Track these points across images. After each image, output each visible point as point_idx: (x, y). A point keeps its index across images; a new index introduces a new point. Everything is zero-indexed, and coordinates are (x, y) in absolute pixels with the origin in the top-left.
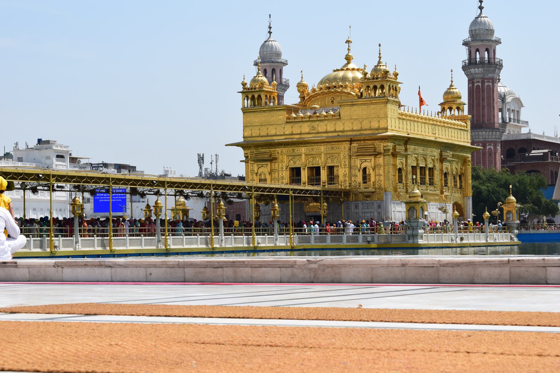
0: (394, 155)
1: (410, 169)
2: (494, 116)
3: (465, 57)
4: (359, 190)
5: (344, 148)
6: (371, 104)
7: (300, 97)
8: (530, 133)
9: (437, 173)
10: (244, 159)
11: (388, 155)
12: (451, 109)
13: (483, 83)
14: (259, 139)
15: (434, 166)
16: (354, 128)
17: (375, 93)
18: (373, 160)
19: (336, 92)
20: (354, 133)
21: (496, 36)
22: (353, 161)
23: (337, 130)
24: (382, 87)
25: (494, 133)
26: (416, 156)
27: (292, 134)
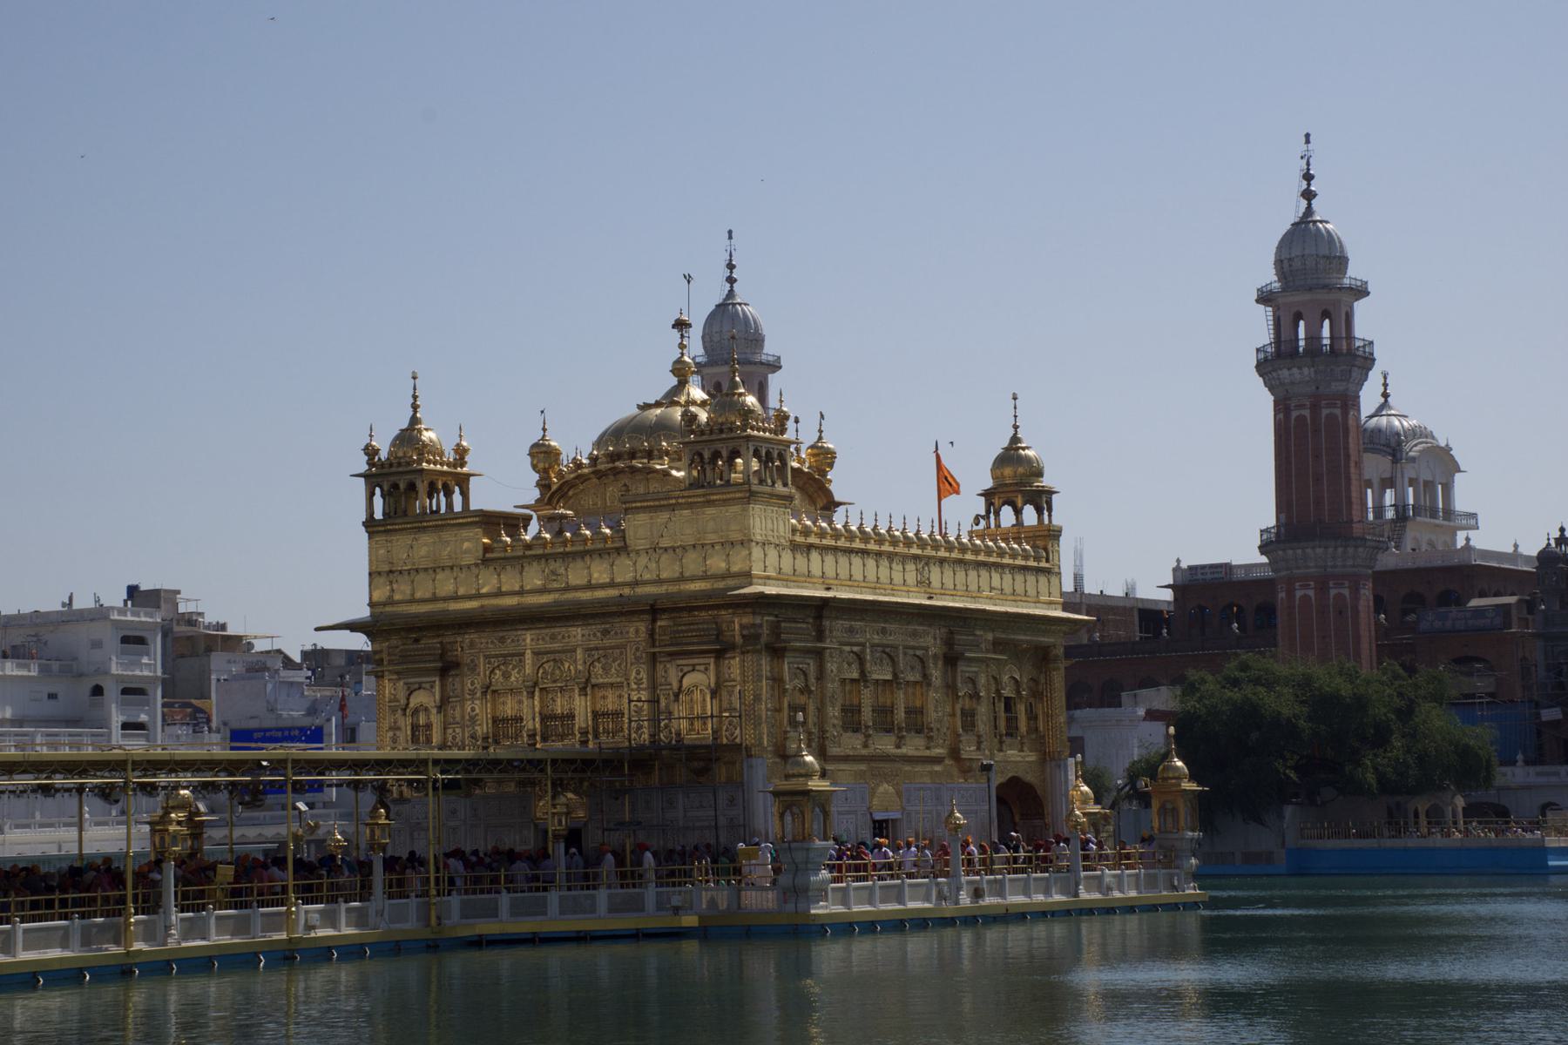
0: (777, 651)
2: (1350, 503)
5: (637, 631)
6: (710, 503)
7: (538, 485)
8: (1468, 547)
11: (759, 652)
13: (1315, 408)
14: (586, 596)
15: (925, 676)
16: (664, 575)
18: (712, 667)
19: (633, 470)
20: (662, 589)
22: (660, 667)
23: (618, 580)
25: (1351, 550)
26: (855, 649)
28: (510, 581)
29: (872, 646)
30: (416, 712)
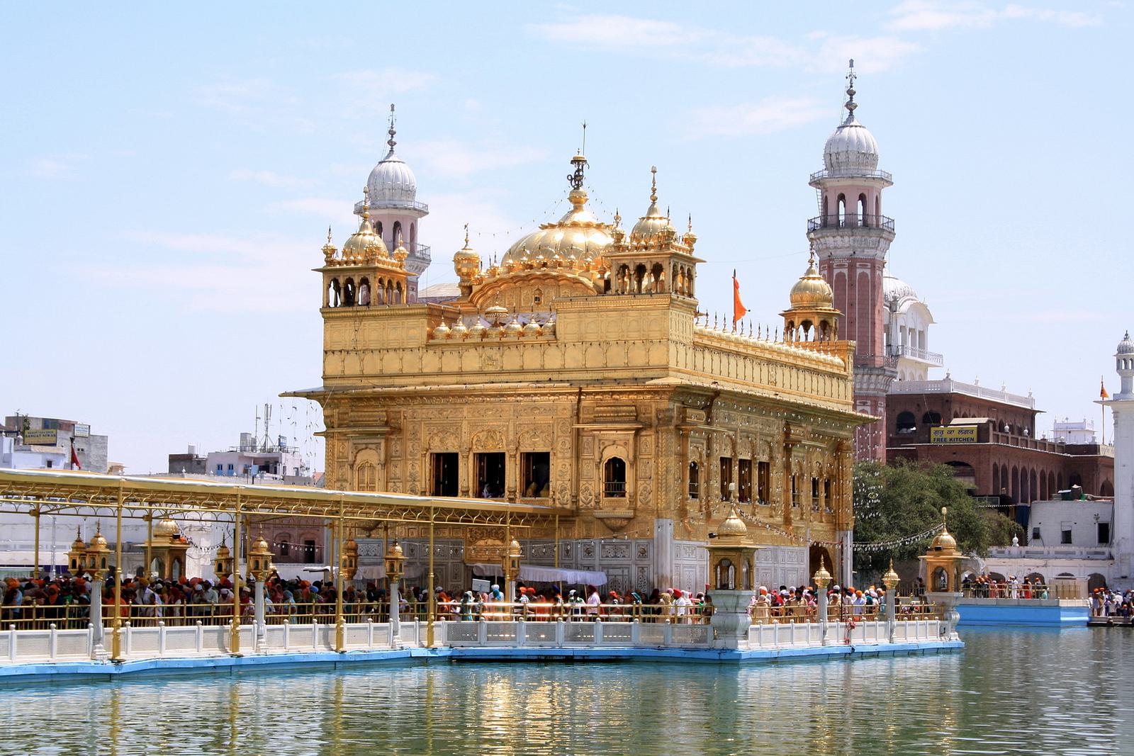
1: (716, 466)
2: (874, 342)
3: (815, 211)
4: (598, 514)
7: (460, 286)
8: (948, 379)
9: (776, 476)
10: (323, 428)
12: (806, 325)
13: (852, 267)
17: (640, 282)
21: (882, 167)
24: (657, 270)
25: (873, 377)
26: (731, 433)
27: (440, 373)
28: (451, 362)
29: (742, 431)
30: (361, 468)
